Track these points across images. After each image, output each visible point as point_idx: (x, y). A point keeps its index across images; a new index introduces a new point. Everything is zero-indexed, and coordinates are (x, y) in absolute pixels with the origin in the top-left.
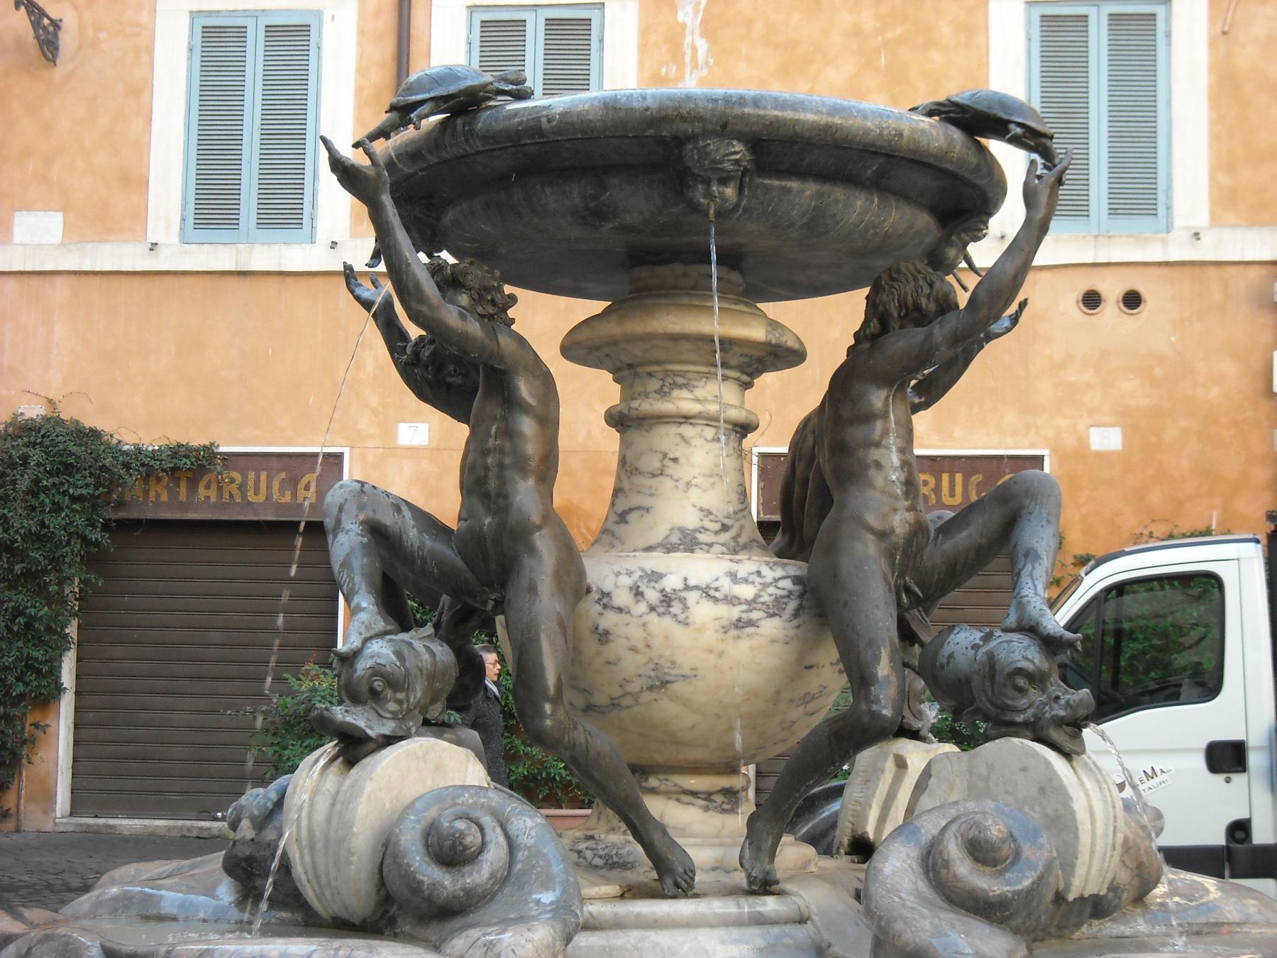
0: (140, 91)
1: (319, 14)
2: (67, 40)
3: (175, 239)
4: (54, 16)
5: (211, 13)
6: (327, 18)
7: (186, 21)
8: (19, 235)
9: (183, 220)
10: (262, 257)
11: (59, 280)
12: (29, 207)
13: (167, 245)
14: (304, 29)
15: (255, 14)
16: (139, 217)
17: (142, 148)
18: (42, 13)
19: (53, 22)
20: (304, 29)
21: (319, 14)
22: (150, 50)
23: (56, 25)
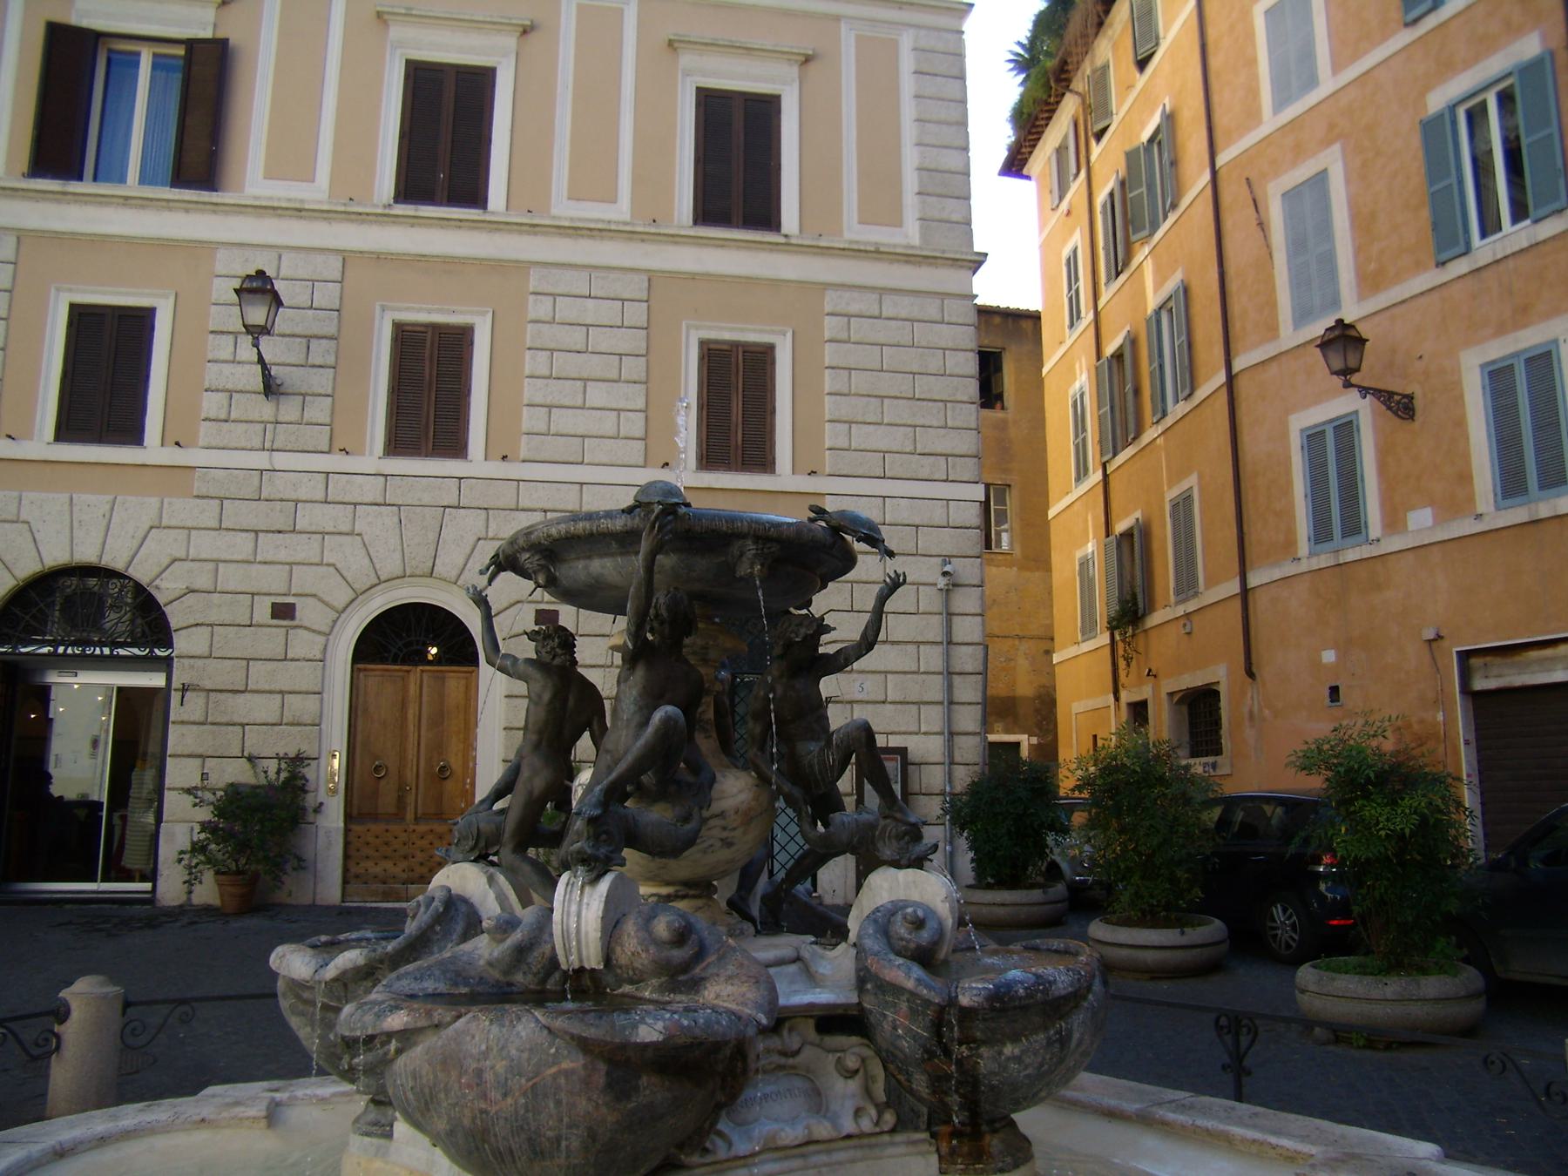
0: (1460, 423)
1: (1555, 342)
2: (1418, 404)
3: (1492, 508)
4: (1408, 391)
5: (1493, 362)
6: (1561, 342)
7: (1478, 371)
8: (1411, 526)
9: (1495, 495)
10: (1544, 510)
11: (1435, 549)
12: (1413, 508)
13: (1487, 514)
14: (1549, 353)
15: (1516, 355)
16: (1471, 499)
17: (1466, 456)
18: (1391, 394)
19: (1405, 396)
20: (1549, 353)
21: (1555, 342)
22: (1461, 396)
23: (1410, 397)
